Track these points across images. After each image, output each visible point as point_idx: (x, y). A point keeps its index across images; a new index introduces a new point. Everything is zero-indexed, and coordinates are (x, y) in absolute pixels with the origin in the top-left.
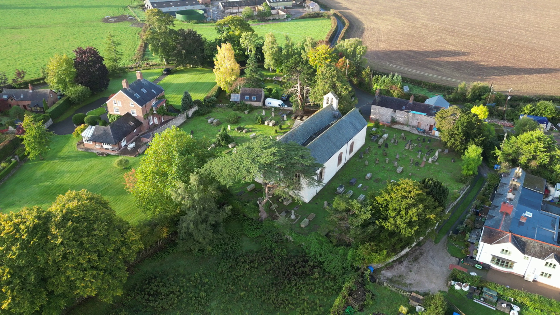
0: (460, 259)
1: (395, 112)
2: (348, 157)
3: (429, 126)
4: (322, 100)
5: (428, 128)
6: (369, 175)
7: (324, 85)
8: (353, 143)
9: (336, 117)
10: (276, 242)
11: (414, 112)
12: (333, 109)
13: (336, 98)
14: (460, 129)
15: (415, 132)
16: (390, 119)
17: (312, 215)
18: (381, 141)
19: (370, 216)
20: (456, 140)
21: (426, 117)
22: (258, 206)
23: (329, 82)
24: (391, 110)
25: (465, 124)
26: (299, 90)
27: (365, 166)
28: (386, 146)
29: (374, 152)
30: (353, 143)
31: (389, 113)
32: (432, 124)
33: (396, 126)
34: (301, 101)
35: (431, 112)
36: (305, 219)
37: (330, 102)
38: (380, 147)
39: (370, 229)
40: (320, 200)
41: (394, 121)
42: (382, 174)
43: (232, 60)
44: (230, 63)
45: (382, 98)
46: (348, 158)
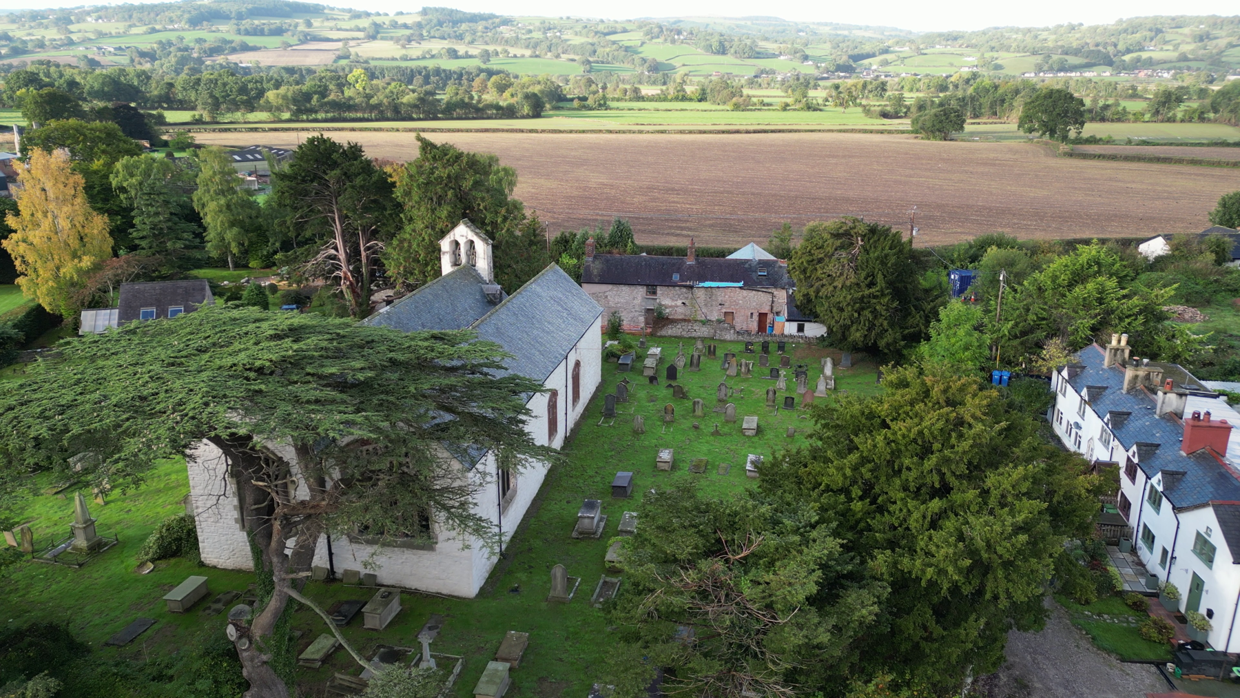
0: (1160, 665)
1: (655, 293)
2: (574, 414)
3: (756, 317)
5: (754, 326)
6: (665, 455)
7: (433, 211)
8: (578, 364)
9: (492, 302)
11: (708, 284)
12: (478, 279)
13: (484, 240)
14: (880, 277)
15: (730, 336)
16: (642, 319)
17: (515, 638)
18: (650, 362)
20: (874, 312)
21: (745, 293)
22: (232, 654)
23: (450, 193)
24: (640, 292)
25: (893, 260)
26: (342, 255)
27: (637, 433)
28: (672, 373)
29: (642, 394)
30: (578, 364)
31: (638, 301)
32: (766, 309)
33: (669, 331)
34: (354, 292)
35: (754, 276)
36: (492, 665)
38: (652, 379)
39: (863, 606)
40: (523, 576)
41: (658, 319)
42: (705, 448)
43: (79, 200)
44: (67, 209)
45: (607, 261)
46: (571, 425)
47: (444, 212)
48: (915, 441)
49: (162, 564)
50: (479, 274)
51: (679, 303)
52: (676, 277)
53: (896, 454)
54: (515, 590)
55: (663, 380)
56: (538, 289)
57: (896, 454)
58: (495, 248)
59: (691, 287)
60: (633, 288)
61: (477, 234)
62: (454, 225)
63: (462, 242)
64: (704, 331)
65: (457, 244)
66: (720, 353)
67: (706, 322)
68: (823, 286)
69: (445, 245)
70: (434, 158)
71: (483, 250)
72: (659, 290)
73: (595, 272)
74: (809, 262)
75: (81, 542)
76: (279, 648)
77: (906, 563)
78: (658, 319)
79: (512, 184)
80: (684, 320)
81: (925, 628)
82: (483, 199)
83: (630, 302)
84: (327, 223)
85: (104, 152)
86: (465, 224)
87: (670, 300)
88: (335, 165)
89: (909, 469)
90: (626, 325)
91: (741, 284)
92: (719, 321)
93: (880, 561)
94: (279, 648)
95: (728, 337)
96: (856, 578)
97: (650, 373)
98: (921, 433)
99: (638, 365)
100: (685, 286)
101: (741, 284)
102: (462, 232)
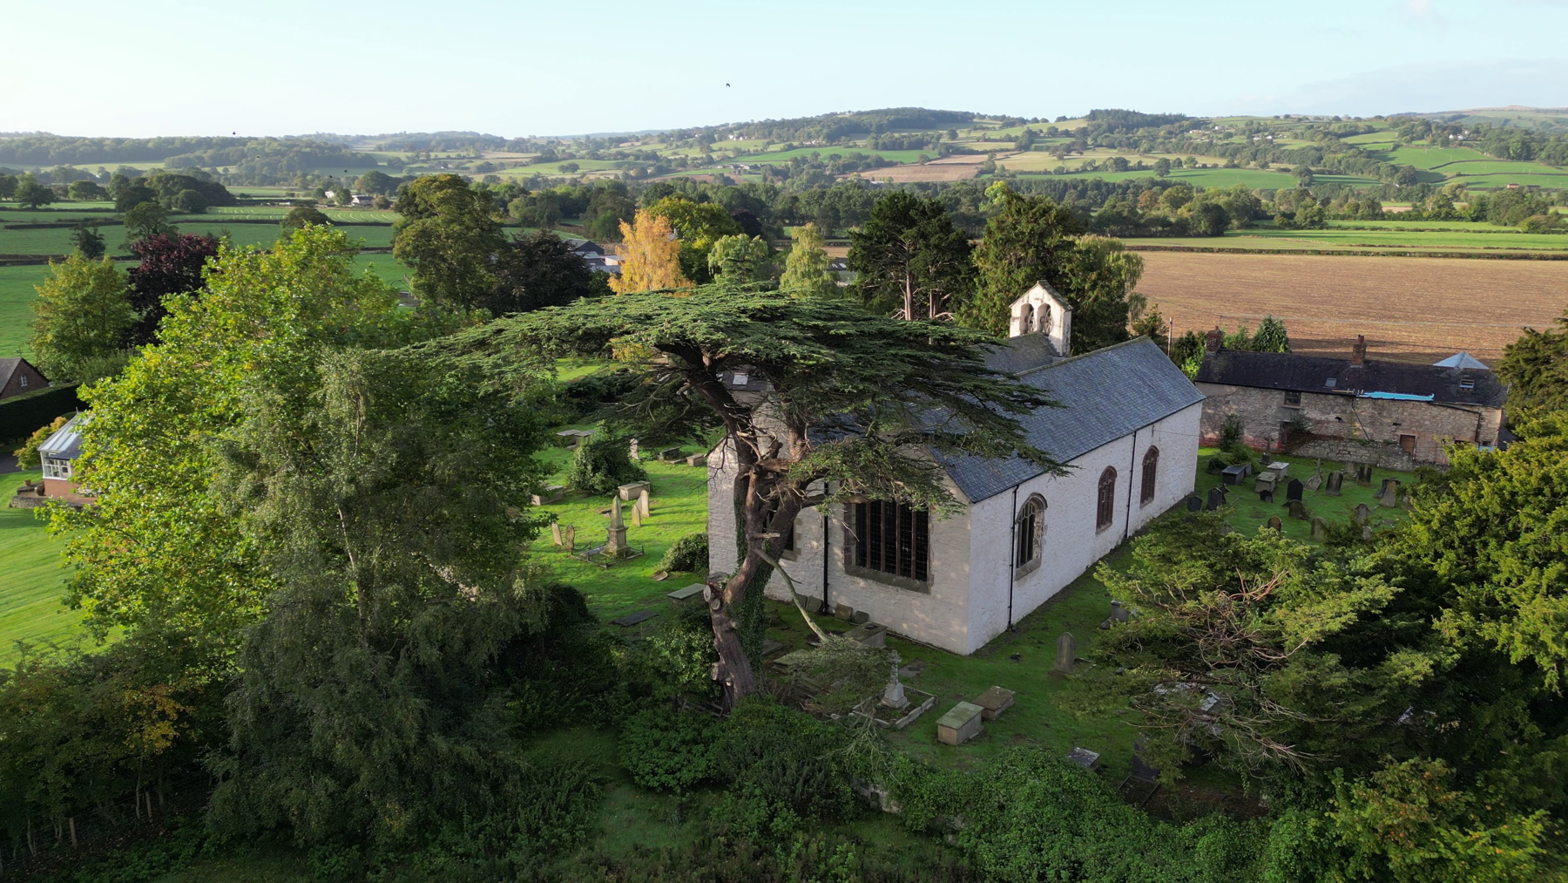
1: (1297, 402)
2: (1140, 515)
4: (1006, 316)
8: (1153, 453)
10: (801, 809)
13: (1063, 305)
16: (1275, 435)
18: (1264, 476)
19: (1384, 593)
21: (1435, 410)
24: (1277, 399)
28: (1295, 489)
30: (1153, 453)
31: (1272, 411)
33: (1310, 450)
35: (1453, 389)
37: (1036, 327)
38: (1265, 495)
40: (1029, 649)
41: (1296, 435)
43: (672, 265)
44: (660, 272)
47: (1020, 276)
48: (1539, 492)
49: (677, 574)
50: (1051, 346)
51: (1332, 417)
52: (1331, 383)
53: (1510, 504)
54: (1016, 658)
55: (1281, 498)
56: (1116, 358)
57: (1510, 504)
58: (1074, 318)
59: (1352, 397)
60: (1266, 392)
61: (1055, 298)
62: (1026, 288)
63: (1036, 306)
64: (1364, 455)
65: (1031, 309)
66: (1377, 480)
67: (1364, 444)
68: (1549, 394)
69: (1016, 309)
70: (1018, 212)
71: (1058, 313)
72: (1304, 398)
73: (1216, 370)
74: (1527, 361)
75: (613, 548)
76: (747, 618)
77: (1488, 630)
78: (1296, 435)
79: (1135, 275)
80: (1335, 438)
81: (1515, 726)
82: (1070, 260)
83: (1260, 412)
84: (898, 290)
85: (706, 232)
86: (1043, 286)
87: (1317, 412)
88: (912, 223)
89: (1528, 530)
90: (1248, 435)
91: (1430, 398)
92: (1387, 443)
93: (1447, 624)
94: (747, 618)
95: (1398, 465)
96: (1419, 639)
97: (1267, 488)
98: (1546, 479)
99: (1251, 481)
100: (1342, 395)
101: (1430, 398)
102: (1038, 295)
